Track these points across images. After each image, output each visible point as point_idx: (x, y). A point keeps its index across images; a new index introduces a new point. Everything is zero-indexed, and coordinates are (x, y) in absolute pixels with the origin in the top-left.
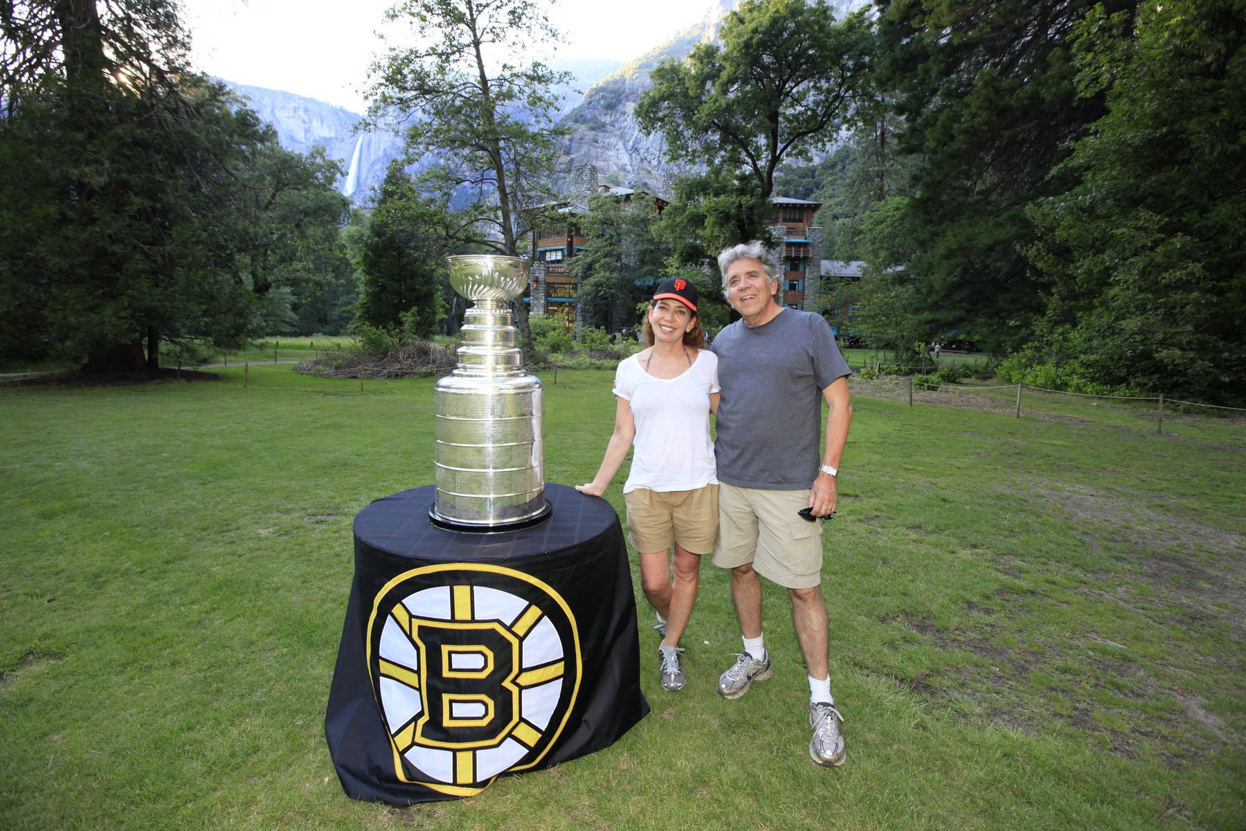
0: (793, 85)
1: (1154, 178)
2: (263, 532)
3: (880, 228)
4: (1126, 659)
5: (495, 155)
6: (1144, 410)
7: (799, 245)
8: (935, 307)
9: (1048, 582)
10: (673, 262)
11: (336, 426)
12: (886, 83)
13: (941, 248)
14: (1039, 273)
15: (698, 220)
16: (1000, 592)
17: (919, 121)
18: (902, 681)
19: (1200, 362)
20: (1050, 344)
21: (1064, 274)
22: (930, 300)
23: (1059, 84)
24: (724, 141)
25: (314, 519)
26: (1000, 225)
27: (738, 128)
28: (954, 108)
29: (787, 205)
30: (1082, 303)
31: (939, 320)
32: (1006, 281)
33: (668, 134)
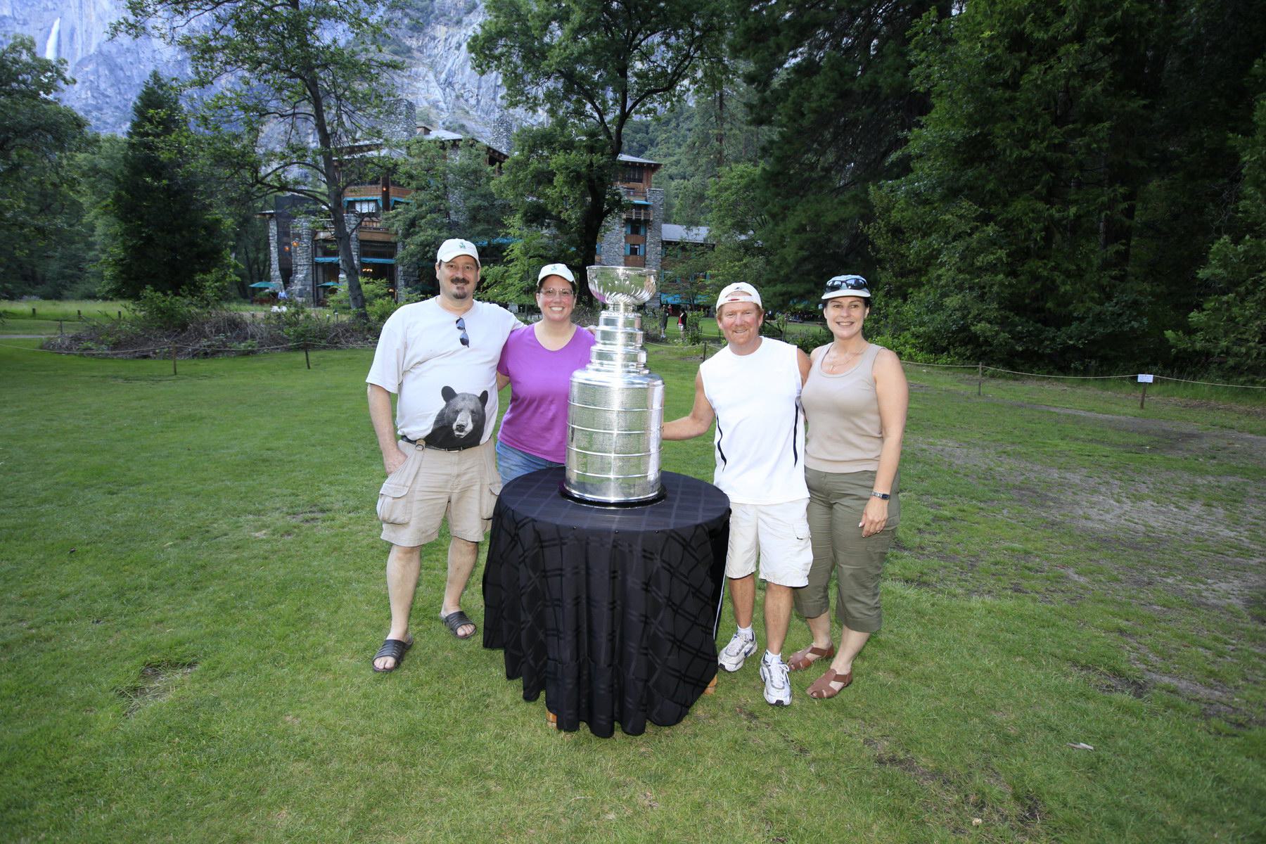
0: (642, 37)
1: (970, 173)
2: (260, 535)
3: (725, 194)
4: (1027, 553)
5: (312, 84)
6: (962, 375)
7: (639, 207)
8: (786, 279)
9: (960, 510)
10: (515, 222)
11: (191, 418)
12: (740, 51)
13: (792, 223)
14: (878, 251)
15: (545, 178)
16: (933, 520)
17: (768, 92)
18: (907, 582)
19: (1002, 334)
20: (886, 317)
21: (898, 252)
22: (782, 273)
23: (893, 75)
24: (568, 90)
25: (301, 517)
26: (843, 203)
27: (584, 77)
28: (803, 86)
29: (627, 162)
30: (911, 279)
31: (791, 293)
32: (847, 255)
33: (505, 75)
